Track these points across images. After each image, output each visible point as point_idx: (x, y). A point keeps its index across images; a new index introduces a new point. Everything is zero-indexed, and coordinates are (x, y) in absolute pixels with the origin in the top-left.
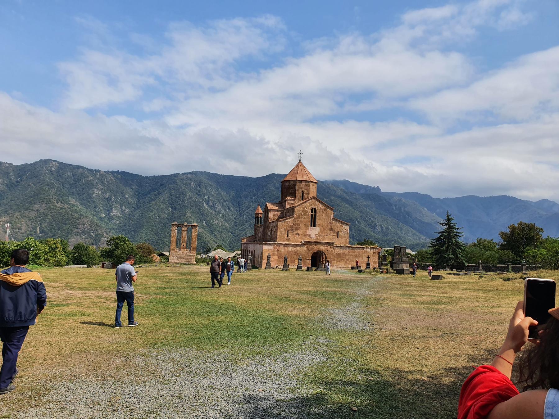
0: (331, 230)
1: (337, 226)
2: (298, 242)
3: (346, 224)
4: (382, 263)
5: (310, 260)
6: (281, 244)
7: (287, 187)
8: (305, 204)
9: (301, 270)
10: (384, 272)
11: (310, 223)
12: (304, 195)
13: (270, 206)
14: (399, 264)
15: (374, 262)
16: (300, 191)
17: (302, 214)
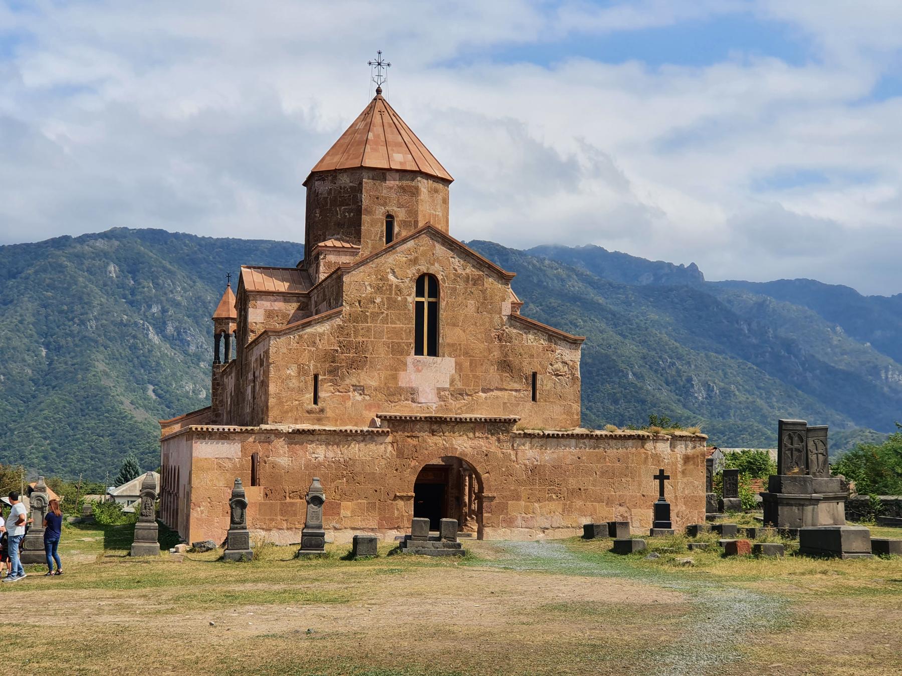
0: (505, 365)
1: (529, 347)
2: (363, 422)
3: (565, 339)
4: (721, 503)
5: (408, 498)
6: (277, 434)
7: (325, 199)
8: (390, 259)
9: (319, 556)
10: (742, 551)
11: (412, 340)
12: (396, 229)
13: (253, 280)
14: (801, 503)
15: (690, 501)
16: (380, 213)
17: (378, 300)
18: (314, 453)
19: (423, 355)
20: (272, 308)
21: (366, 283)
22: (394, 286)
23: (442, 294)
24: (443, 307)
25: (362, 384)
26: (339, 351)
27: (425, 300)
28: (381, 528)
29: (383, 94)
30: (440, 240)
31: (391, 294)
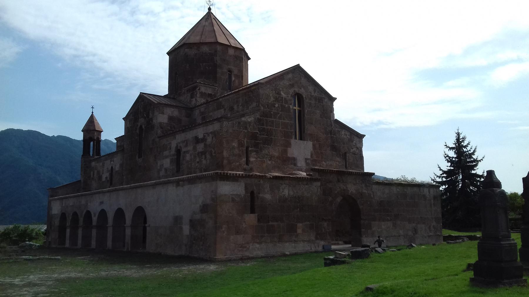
0: (334, 148)
12: (233, 79)
17: (277, 106)
18: (283, 192)
19: (296, 139)
20: (172, 115)
21: (271, 95)
22: (284, 99)
23: (305, 106)
24: (306, 113)
25: (270, 154)
26: (259, 133)
27: (297, 108)
28: (317, 238)
29: (212, 11)
30: (303, 75)
31: (283, 103)
